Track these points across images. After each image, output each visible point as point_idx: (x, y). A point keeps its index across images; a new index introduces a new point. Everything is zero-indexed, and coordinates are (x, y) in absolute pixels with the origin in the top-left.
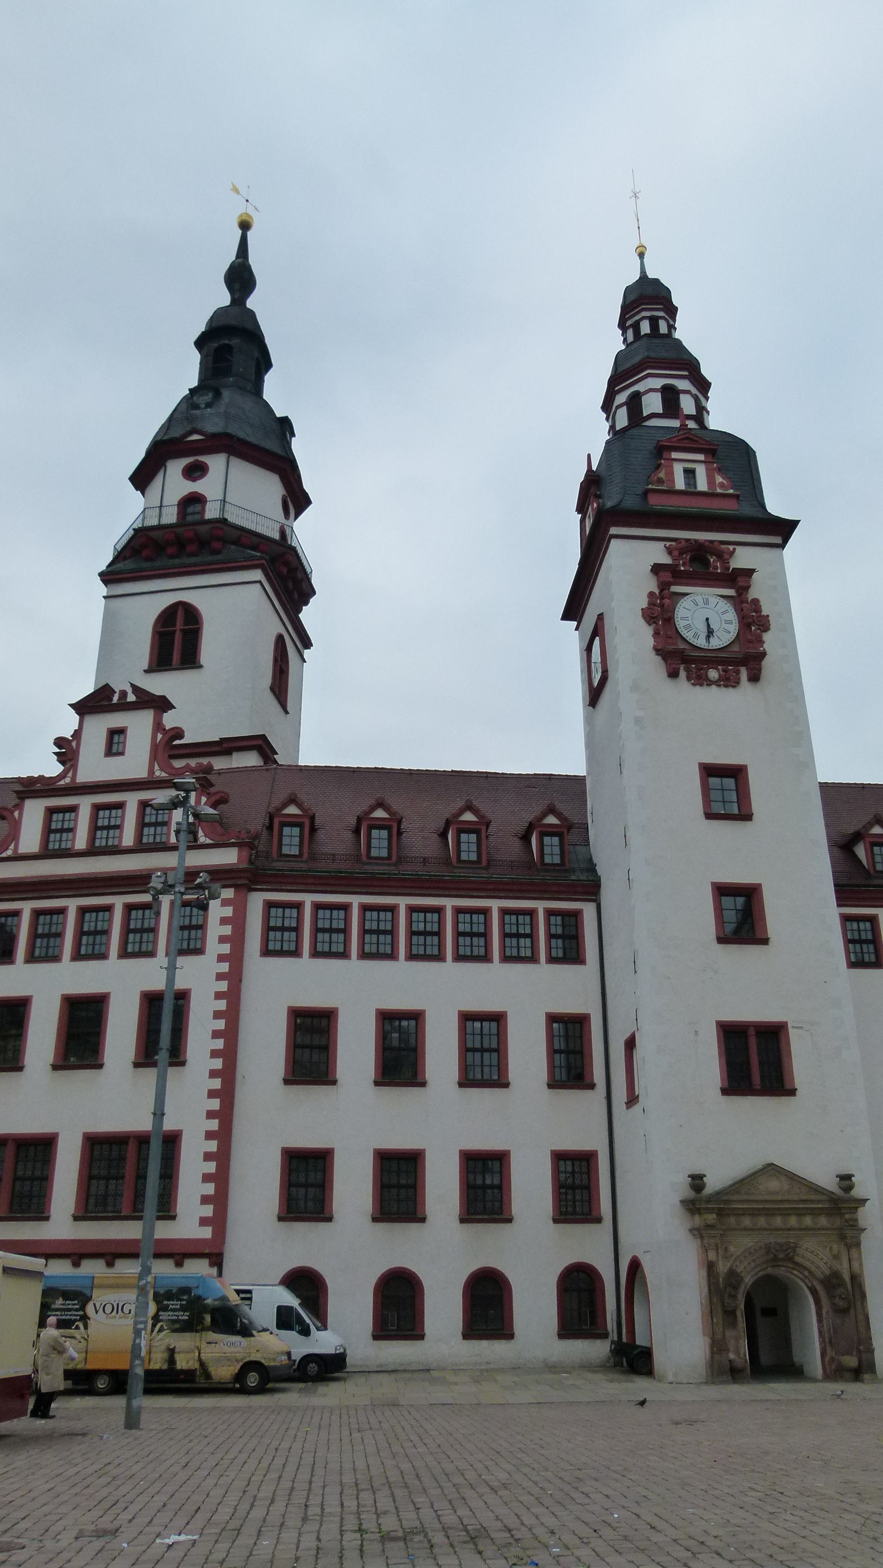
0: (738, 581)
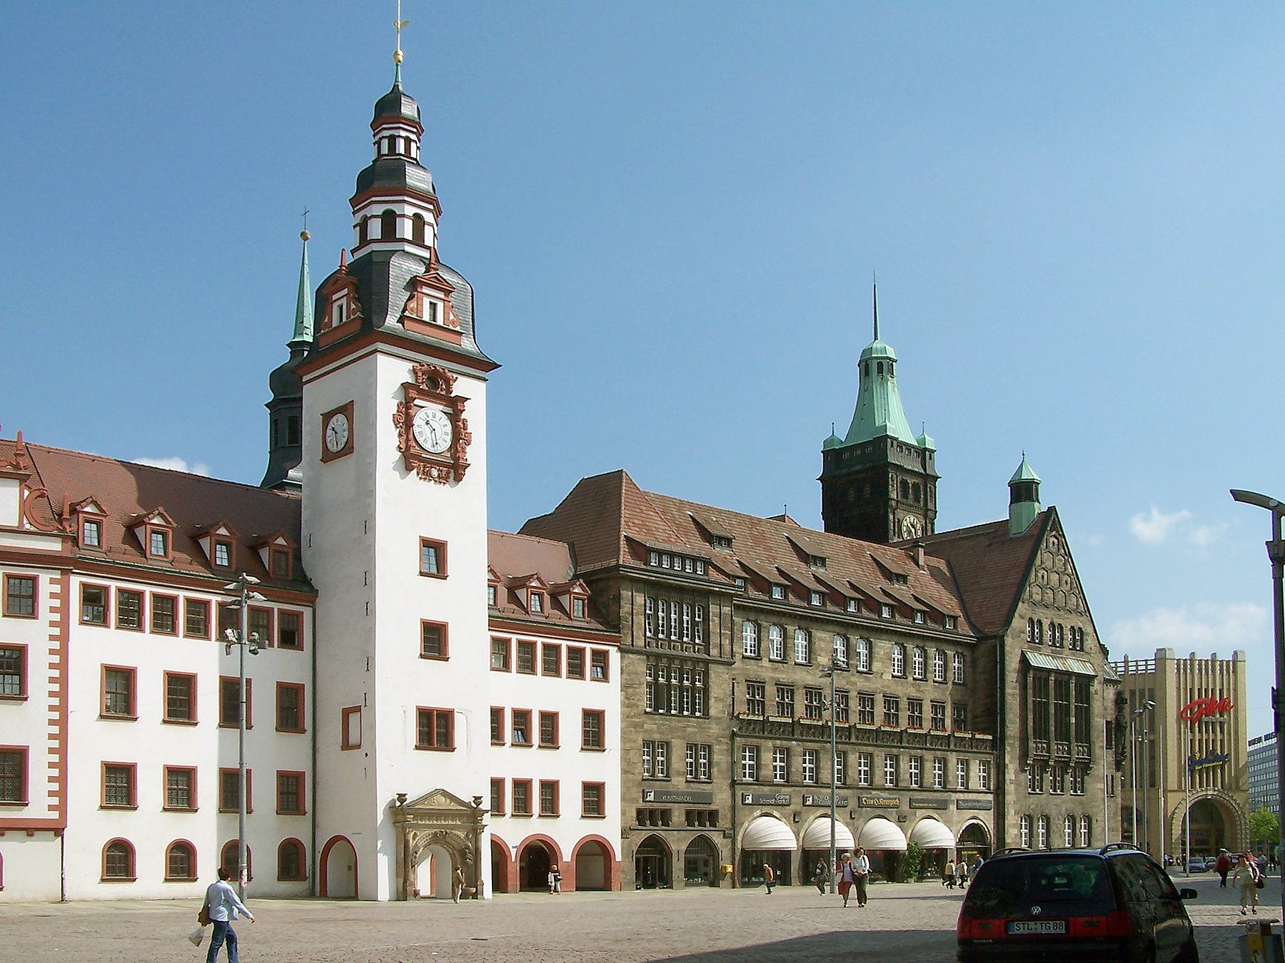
0: (455, 407)
